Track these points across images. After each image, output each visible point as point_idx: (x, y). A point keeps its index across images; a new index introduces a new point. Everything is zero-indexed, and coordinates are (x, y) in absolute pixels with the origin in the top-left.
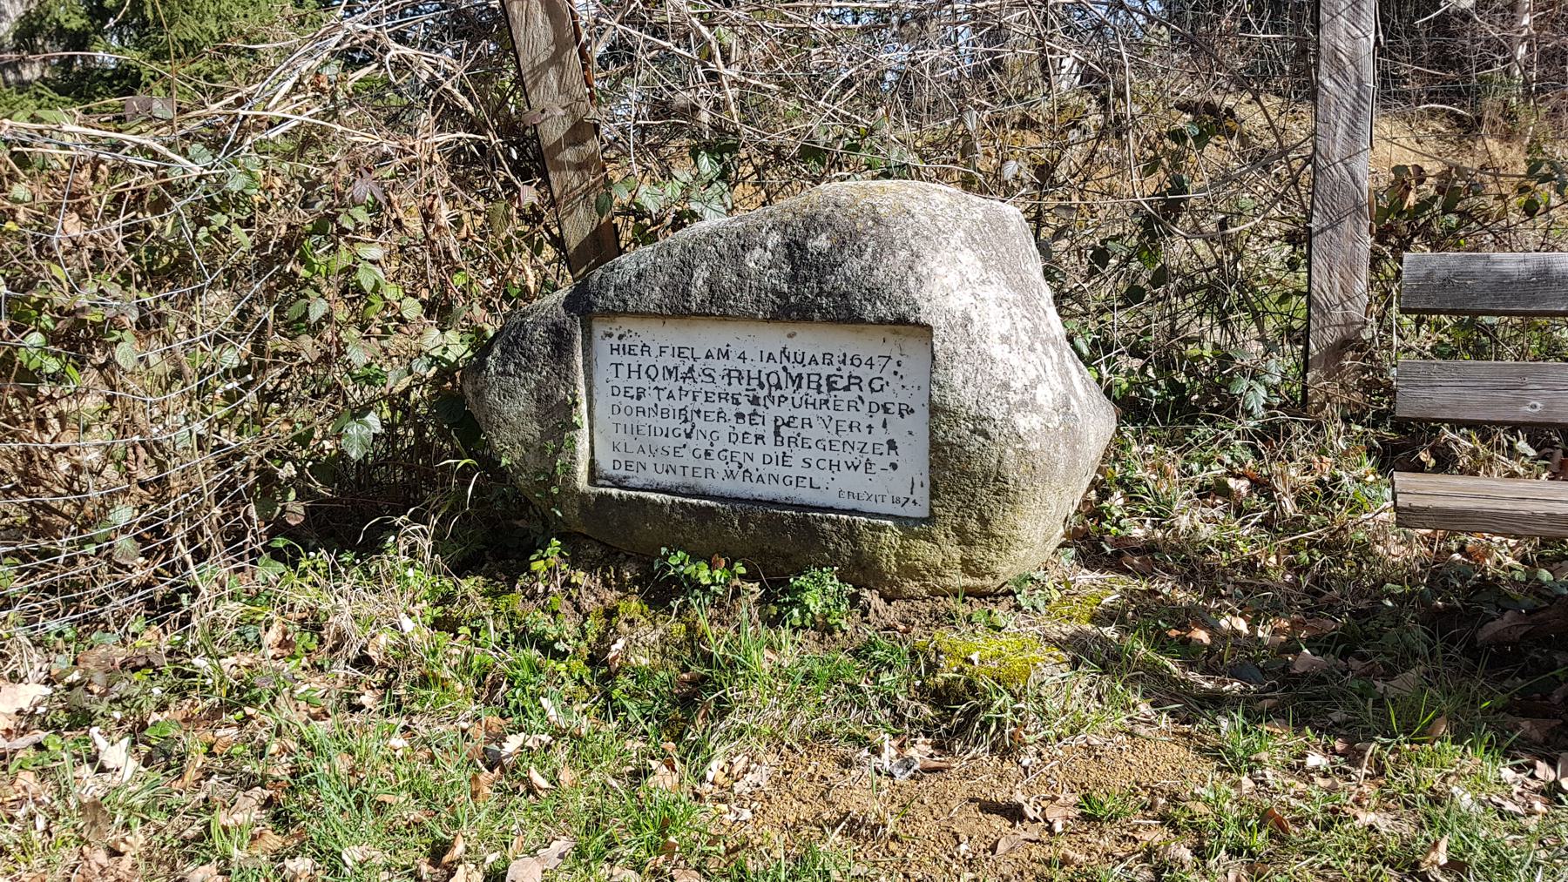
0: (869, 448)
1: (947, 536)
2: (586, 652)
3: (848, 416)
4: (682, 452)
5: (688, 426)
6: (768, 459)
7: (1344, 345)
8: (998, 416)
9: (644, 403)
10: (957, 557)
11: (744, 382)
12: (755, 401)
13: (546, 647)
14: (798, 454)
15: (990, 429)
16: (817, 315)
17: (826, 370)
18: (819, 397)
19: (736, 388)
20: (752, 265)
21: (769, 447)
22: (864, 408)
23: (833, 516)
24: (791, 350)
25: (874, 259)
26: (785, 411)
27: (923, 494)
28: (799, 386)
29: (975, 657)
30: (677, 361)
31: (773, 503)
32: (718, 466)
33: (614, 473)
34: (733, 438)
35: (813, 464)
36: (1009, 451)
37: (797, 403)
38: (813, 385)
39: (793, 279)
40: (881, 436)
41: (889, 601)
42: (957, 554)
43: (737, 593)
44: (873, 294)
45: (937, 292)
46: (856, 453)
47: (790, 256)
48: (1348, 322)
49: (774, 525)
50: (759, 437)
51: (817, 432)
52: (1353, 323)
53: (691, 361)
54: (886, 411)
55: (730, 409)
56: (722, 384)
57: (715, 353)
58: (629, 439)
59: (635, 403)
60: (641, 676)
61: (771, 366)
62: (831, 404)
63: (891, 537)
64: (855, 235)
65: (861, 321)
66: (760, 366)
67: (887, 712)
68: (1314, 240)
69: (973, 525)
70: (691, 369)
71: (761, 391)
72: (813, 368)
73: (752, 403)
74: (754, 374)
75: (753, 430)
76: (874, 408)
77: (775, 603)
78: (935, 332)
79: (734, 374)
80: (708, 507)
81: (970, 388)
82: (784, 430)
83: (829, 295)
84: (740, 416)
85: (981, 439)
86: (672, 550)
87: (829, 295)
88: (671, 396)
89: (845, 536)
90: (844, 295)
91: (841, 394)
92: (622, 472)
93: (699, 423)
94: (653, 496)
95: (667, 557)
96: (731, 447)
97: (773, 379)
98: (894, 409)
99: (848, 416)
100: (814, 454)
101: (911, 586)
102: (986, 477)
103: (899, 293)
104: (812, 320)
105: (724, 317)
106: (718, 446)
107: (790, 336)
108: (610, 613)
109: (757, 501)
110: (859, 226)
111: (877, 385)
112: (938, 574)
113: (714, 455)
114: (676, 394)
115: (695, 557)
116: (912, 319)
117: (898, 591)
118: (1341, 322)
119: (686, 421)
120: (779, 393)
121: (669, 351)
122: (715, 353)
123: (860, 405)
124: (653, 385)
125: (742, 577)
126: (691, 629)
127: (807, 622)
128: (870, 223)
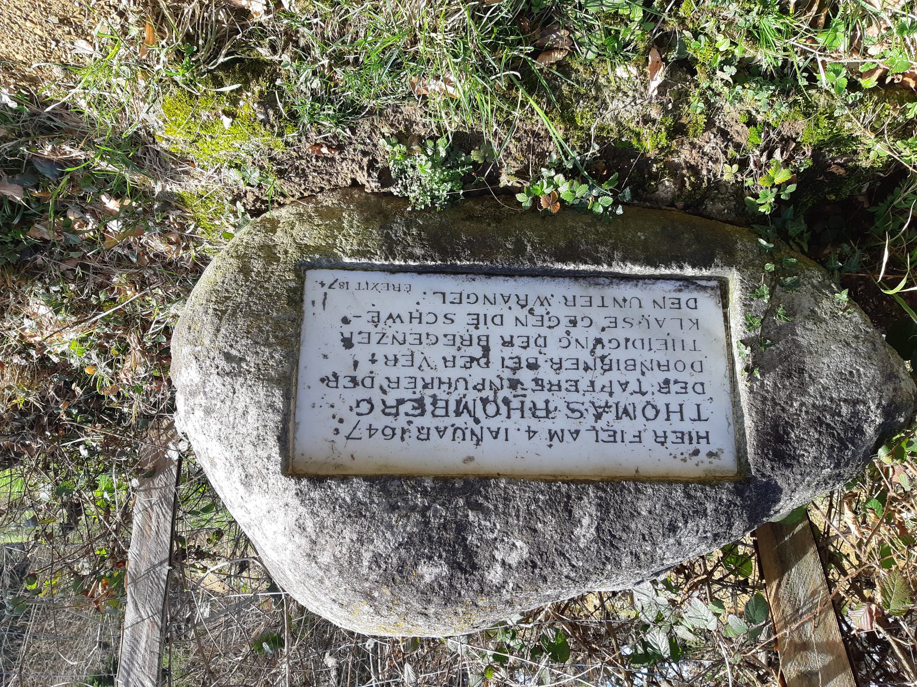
0: (375, 338)
1: (286, 252)
2: (701, 78)
3: (401, 372)
4: (606, 323)
5: (599, 351)
6: (497, 320)
7: (152, 474)
8: (214, 378)
9: (660, 376)
10: (279, 233)
11: (528, 405)
12: (514, 384)
13: (747, 72)
14: (460, 327)
15: (222, 363)
16: (428, 484)
17: (427, 421)
18: (435, 391)
19: (539, 398)
20: (519, 544)
21: (495, 334)
22: (380, 380)
23: (411, 263)
24: (469, 443)
25: (358, 552)
26: (477, 374)
27: (312, 291)
28: (458, 402)
29: (227, 121)
30: (618, 426)
31: (490, 273)
32: (559, 310)
33: (695, 294)
34: (541, 341)
35: (441, 319)
36: (207, 342)
37: (461, 384)
38: (441, 404)
39: (462, 527)
40: (361, 352)
41: (354, 182)
42: (280, 237)
43: (522, 174)
44: (355, 511)
45: (280, 513)
46: (390, 333)
47: (470, 554)
48: (148, 491)
49: (480, 248)
50: (508, 343)
51: (436, 354)
52: (145, 490)
53: (598, 427)
54: (353, 380)
55: (546, 373)
56: (557, 400)
57: (567, 436)
58: (678, 334)
59: (672, 375)
60: (619, 49)
61: (494, 424)
62: (420, 384)
63: (346, 247)
64: (388, 580)
65: (371, 479)
66: (508, 424)
67: (302, 42)
68: (167, 556)
69: (257, 265)
70: (598, 417)
71: (508, 395)
72: (442, 423)
73: (519, 382)
74: (516, 414)
75: (516, 351)
76: (368, 382)
77: (474, 163)
78: (278, 468)
79: (542, 413)
80: (564, 261)
81: (240, 406)
82: (477, 352)
83: (413, 509)
84: (533, 366)
85: (234, 352)
86: (608, 216)
87: (413, 509)
88: (624, 385)
89: (398, 243)
90: (393, 508)
91: (408, 395)
92: (684, 296)
93: (585, 356)
94: (637, 270)
95: (615, 204)
96: (544, 331)
97: (491, 409)
98: (343, 382)
99: (401, 372)
100: (440, 329)
101: (329, 200)
102: (234, 313)
103: (323, 513)
104: (436, 478)
105: (550, 480)
106: (560, 331)
107: (471, 459)
108: (678, 130)
109: (510, 274)
110: (386, 591)
111: (365, 407)
112: (301, 215)
113: (565, 321)
114: (617, 388)
115: (580, 208)
116: (304, 482)
117: (344, 195)
118: (153, 491)
119: (603, 358)
120: (484, 394)
121: (628, 438)
122: (567, 436)
123: (385, 384)
124: (648, 397)
125: (520, 190)
126: (569, 120)
127: (430, 144)
128: (376, 594)
